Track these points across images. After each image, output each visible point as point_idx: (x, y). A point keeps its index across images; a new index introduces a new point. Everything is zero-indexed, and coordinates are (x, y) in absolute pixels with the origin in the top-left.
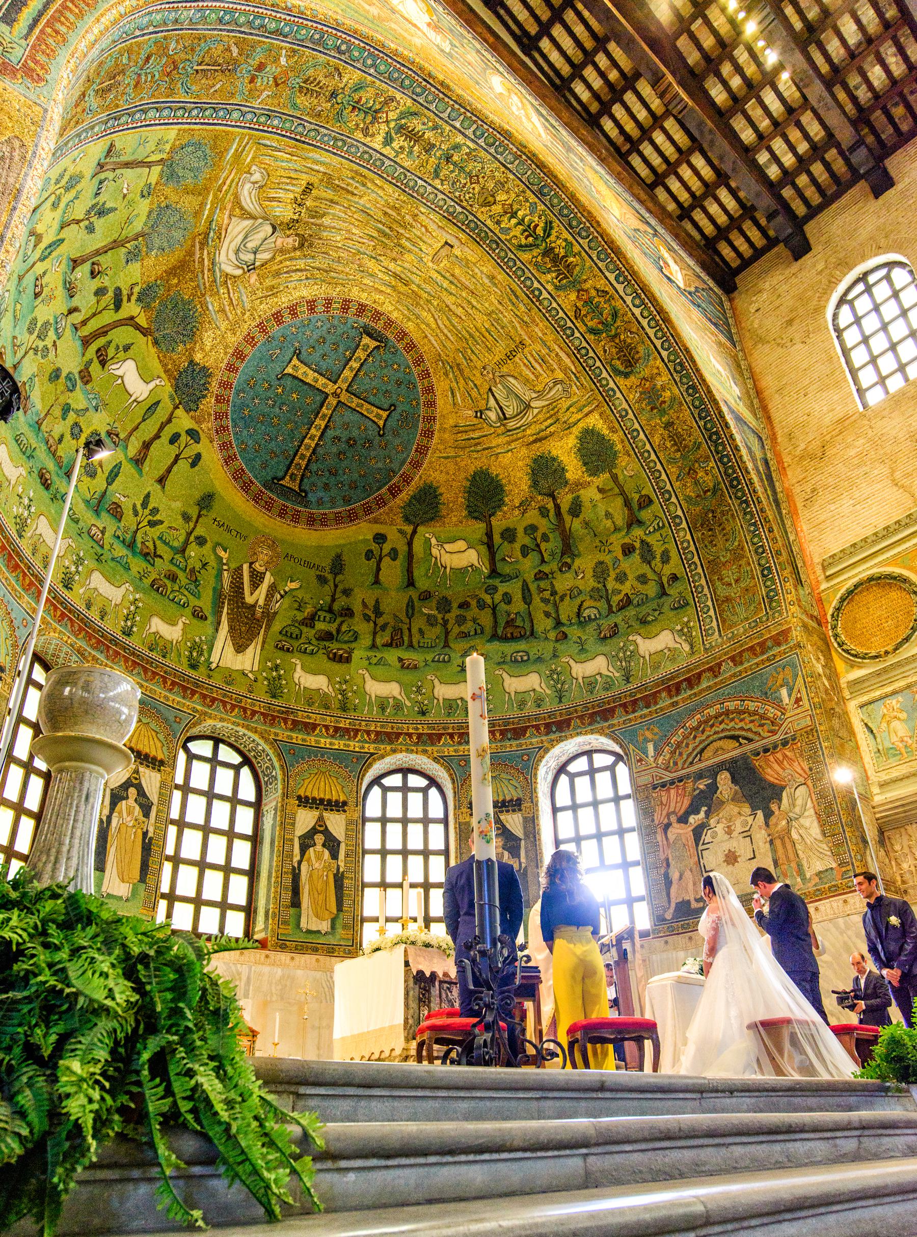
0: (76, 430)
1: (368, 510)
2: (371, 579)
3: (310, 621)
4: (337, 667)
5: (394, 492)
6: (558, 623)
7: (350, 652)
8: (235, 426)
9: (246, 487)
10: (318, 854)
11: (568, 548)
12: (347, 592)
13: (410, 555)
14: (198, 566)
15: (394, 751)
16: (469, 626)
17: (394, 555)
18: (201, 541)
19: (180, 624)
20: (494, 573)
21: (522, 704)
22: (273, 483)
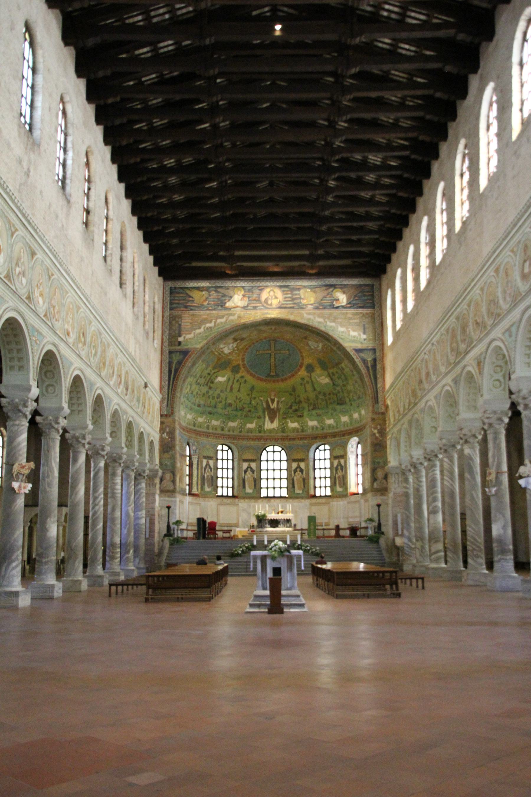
0: (213, 398)
1: (297, 373)
2: (304, 391)
3: (291, 407)
4: (300, 419)
5: (301, 367)
6: (350, 400)
7: (303, 413)
8: (251, 369)
9: (261, 380)
10: (298, 473)
11: (346, 379)
12: (299, 396)
13: (312, 382)
14: (256, 404)
15: (316, 442)
16: (332, 401)
17: (308, 382)
18: (255, 398)
19: (255, 422)
20: (334, 384)
21: (344, 426)
22: (268, 375)
